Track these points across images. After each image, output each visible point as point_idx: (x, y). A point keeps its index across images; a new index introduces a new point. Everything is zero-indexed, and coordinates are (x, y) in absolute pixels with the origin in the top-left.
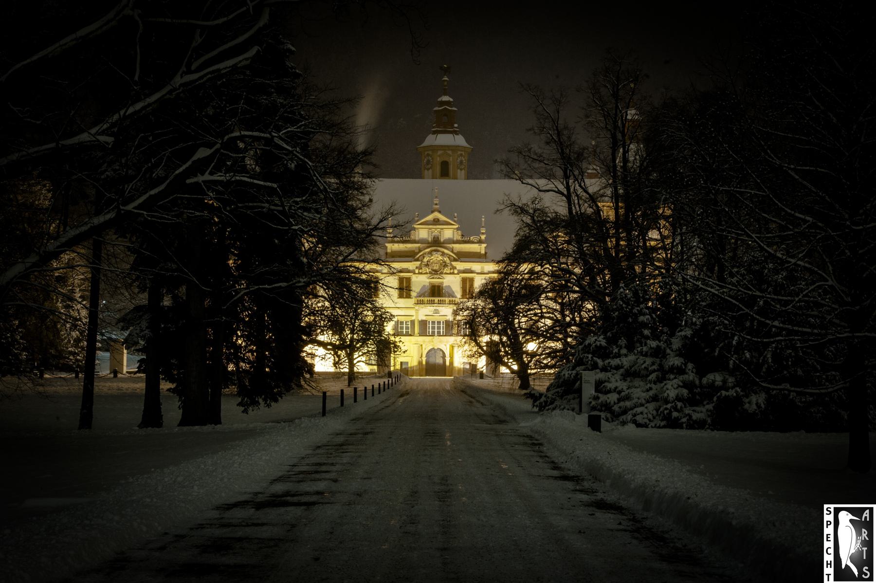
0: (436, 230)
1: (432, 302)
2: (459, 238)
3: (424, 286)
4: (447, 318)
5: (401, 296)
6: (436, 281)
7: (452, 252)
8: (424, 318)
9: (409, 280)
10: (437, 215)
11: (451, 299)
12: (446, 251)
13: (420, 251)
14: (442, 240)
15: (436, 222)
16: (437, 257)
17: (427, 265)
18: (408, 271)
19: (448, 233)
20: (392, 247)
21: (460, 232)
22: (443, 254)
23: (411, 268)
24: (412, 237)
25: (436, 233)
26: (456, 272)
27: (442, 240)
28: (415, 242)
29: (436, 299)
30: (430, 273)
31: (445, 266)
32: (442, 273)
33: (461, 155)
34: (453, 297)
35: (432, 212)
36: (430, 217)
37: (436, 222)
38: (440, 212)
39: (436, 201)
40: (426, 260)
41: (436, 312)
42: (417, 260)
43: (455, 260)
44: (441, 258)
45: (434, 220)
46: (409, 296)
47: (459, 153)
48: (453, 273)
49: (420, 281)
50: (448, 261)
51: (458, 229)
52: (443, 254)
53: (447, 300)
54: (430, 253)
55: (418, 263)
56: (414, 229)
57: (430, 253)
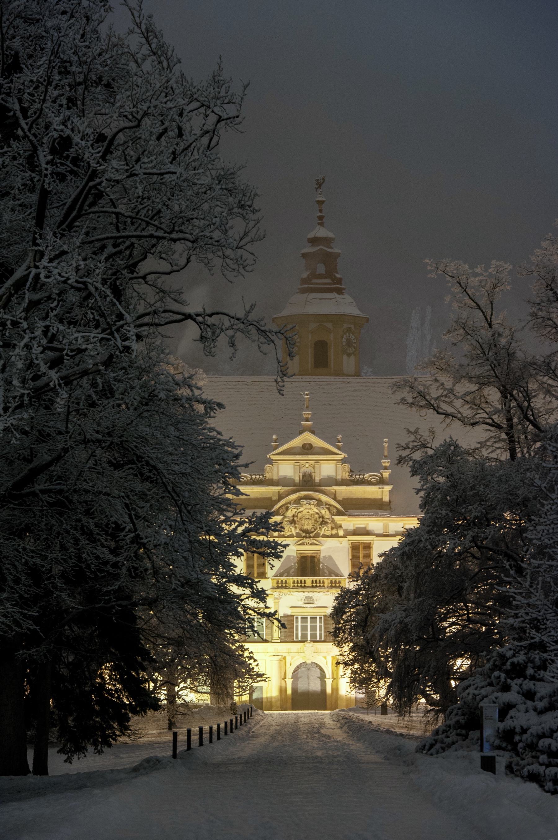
0: (307, 463)
1: (302, 586)
2: (346, 476)
6: (308, 549)
7: (335, 499)
8: (289, 612)
10: (308, 437)
11: (333, 578)
12: (324, 498)
13: (281, 497)
14: (317, 479)
15: (307, 449)
19: (328, 468)
21: (347, 467)
22: (319, 503)
24: (268, 476)
25: (307, 468)
26: (341, 533)
27: (317, 479)
28: (271, 483)
29: (309, 580)
30: (298, 535)
31: (324, 523)
32: (317, 535)
33: (349, 330)
34: (337, 575)
35: (301, 433)
36: (297, 442)
37: (307, 449)
38: (313, 432)
39: (307, 414)
40: (290, 513)
41: (309, 601)
43: (339, 513)
44: (315, 510)
45: (304, 446)
47: (345, 326)
48: (336, 536)
51: (344, 461)
52: (319, 503)
53: (327, 580)
54: (298, 501)
56: (271, 462)
57: (298, 501)
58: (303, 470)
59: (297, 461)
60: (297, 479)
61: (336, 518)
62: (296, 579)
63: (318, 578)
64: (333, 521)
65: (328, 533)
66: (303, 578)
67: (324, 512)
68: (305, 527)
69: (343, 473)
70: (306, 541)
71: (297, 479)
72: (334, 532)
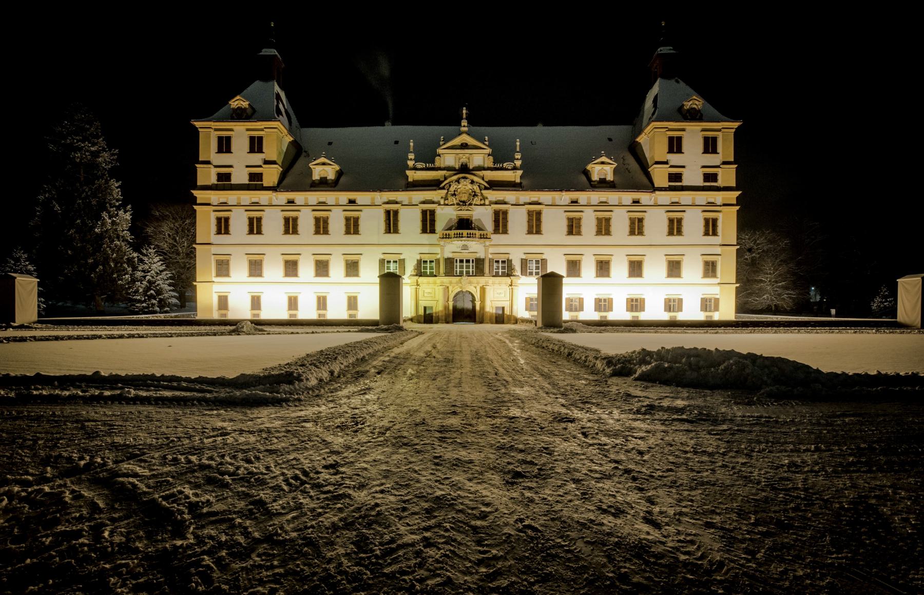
0: (464, 156)
1: (460, 236)
3: (451, 219)
4: (478, 256)
5: (424, 231)
6: (464, 214)
7: (483, 179)
8: (451, 256)
9: (433, 213)
12: (476, 179)
13: (446, 179)
14: (471, 167)
15: (464, 146)
16: (465, 187)
17: (454, 195)
18: (433, 203)
20: (412, 175)
22: (472, 182)
23: (435, 200)
24: (437, 164)
25: (464, 160)
26: (487, 202)
27: (471, 167)
28: (439, 169)
29: (465, 232)
30: (458, 204)
31: (475, 195)
32: (470, 204)
37: (464, 146)
40: (452, 189)
41: (465, 248)
42: (443, 188)
43: (486, 188)
44: (470, 186)
45: (462, 144)
46: (433, 231)
48: (484, 205)
49: (446, 214)
50: (478, 191)
52: (472, 182)
53: (478, 233)
54: (458, 181)
55: (445, 191)
57: (458, 181)
58: (462, 160)
59: (457, 154)
60: (457, 167)
61: (483, 192)
62: (456, 232)
63: (471, 231)
64: (482, 194)
65: (478, 203)
66: (461, 231)
67: (476, 188)
68: (463, 199)
69: (489, 162)
70: (463, 207)
71: (457, 167)
72: (482, 202)
